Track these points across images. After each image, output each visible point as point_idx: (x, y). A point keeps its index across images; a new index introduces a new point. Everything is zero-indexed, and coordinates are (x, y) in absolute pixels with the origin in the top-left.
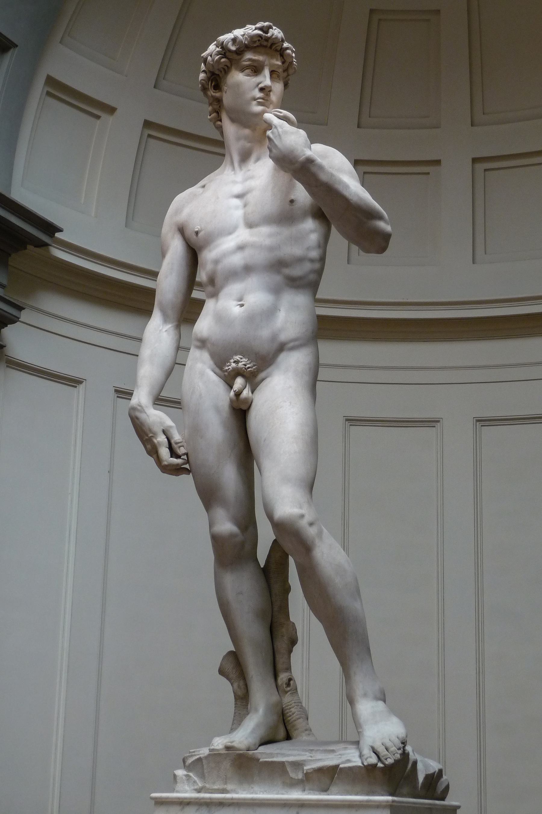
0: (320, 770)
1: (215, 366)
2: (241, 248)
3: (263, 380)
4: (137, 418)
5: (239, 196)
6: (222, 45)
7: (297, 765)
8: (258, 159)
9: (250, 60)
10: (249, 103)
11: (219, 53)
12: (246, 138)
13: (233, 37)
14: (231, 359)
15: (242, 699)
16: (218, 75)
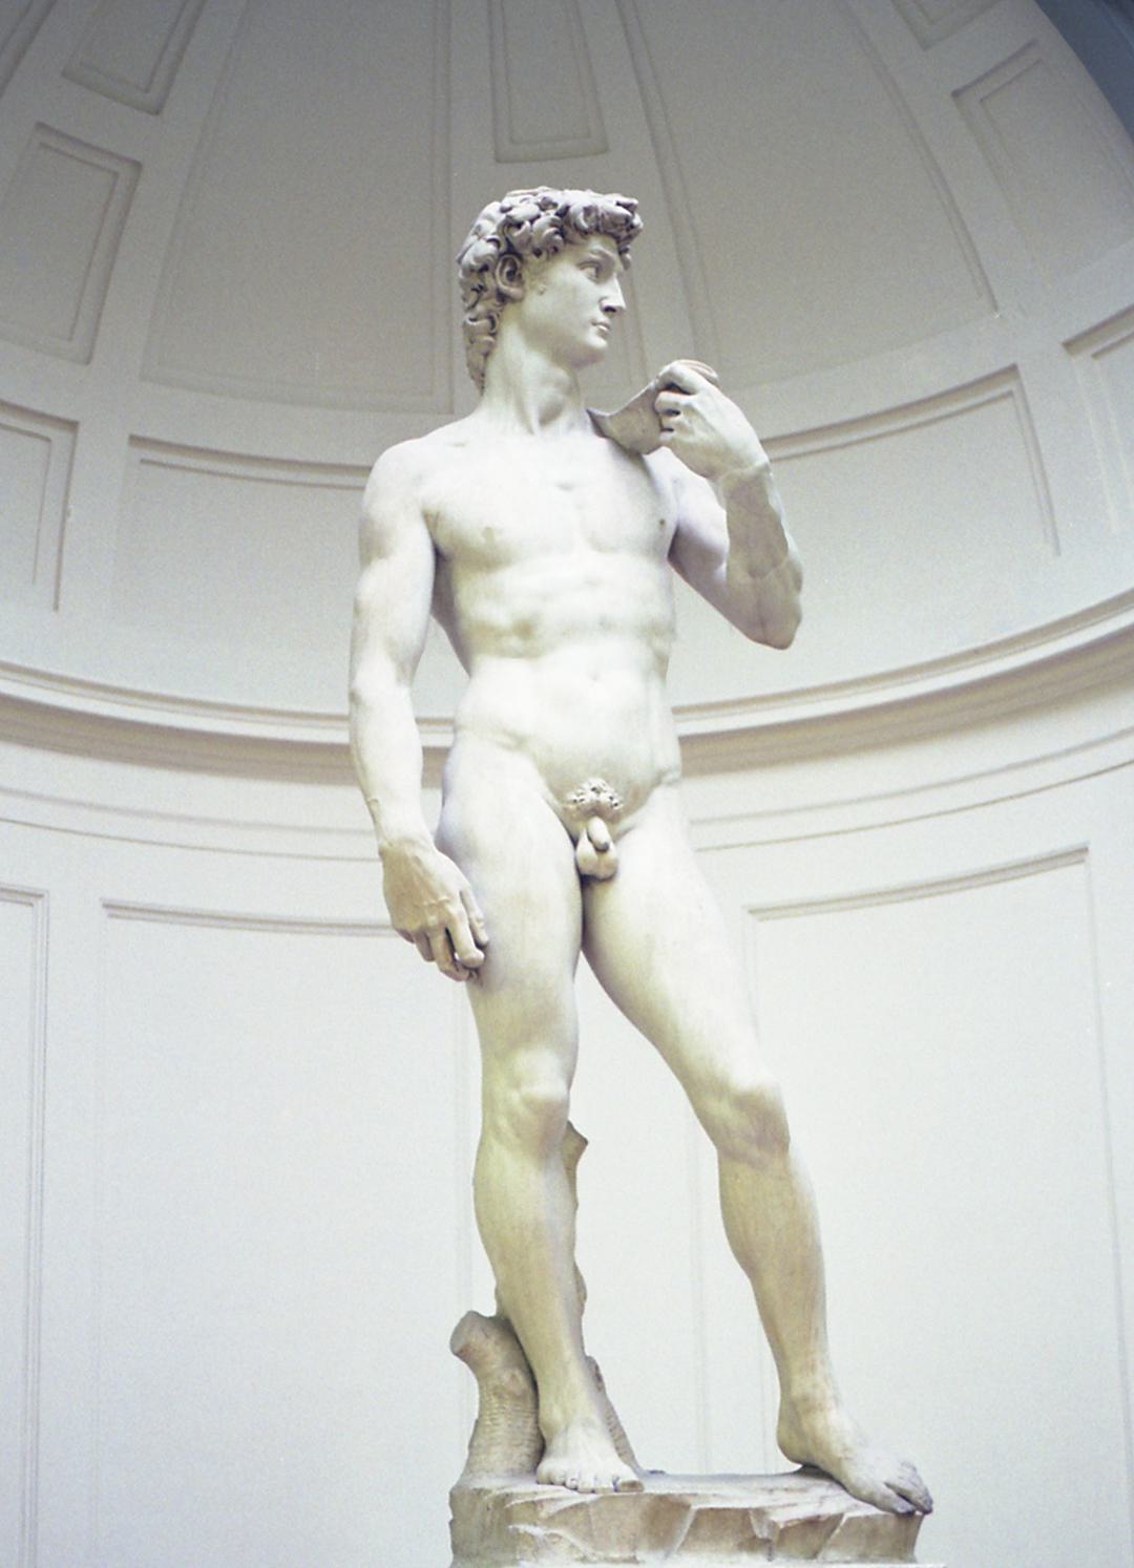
0: (812, 1523)
1: (547, 789)
2: (592, 583)
3: (626, 832)
4: (417, 860)
5: (566, 487)
6: (564, 213)
7: (760, 1512)
8: (571, 426)
9: (600, 253)
10: (585, 327)
11: (553, 224)
12: (558, 384)
13: (587, 203)
14: (582, 782)
15: (516, 1398)
16: (520, 257)
